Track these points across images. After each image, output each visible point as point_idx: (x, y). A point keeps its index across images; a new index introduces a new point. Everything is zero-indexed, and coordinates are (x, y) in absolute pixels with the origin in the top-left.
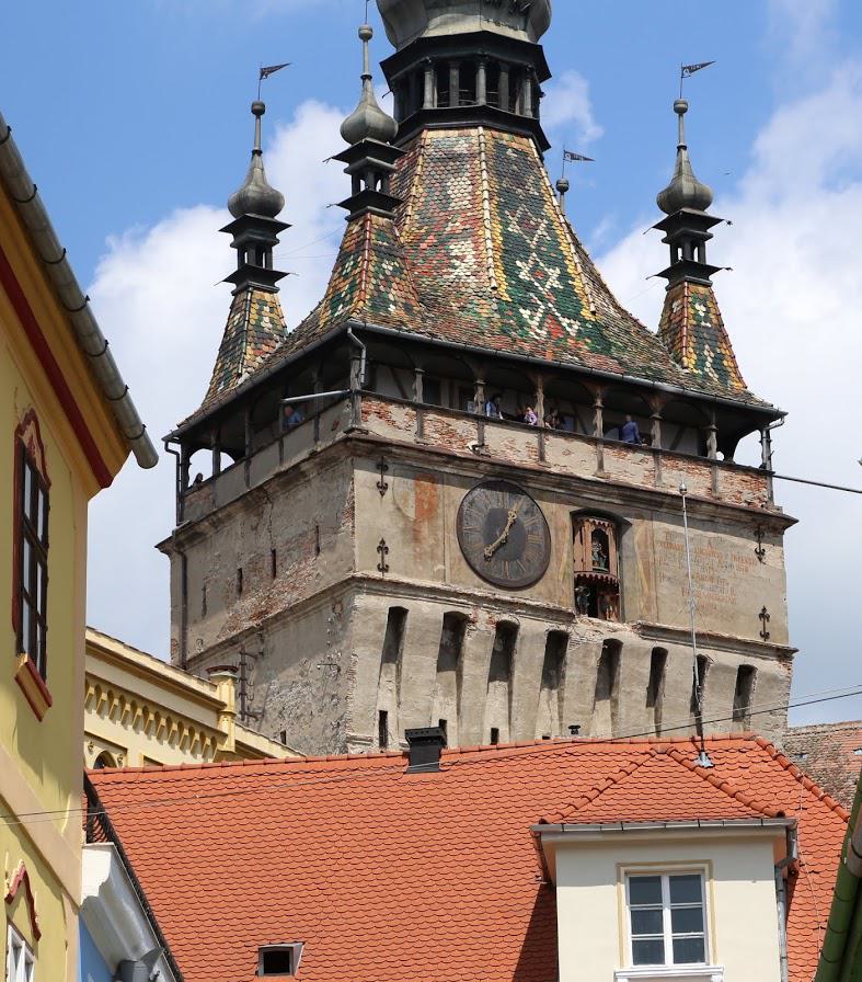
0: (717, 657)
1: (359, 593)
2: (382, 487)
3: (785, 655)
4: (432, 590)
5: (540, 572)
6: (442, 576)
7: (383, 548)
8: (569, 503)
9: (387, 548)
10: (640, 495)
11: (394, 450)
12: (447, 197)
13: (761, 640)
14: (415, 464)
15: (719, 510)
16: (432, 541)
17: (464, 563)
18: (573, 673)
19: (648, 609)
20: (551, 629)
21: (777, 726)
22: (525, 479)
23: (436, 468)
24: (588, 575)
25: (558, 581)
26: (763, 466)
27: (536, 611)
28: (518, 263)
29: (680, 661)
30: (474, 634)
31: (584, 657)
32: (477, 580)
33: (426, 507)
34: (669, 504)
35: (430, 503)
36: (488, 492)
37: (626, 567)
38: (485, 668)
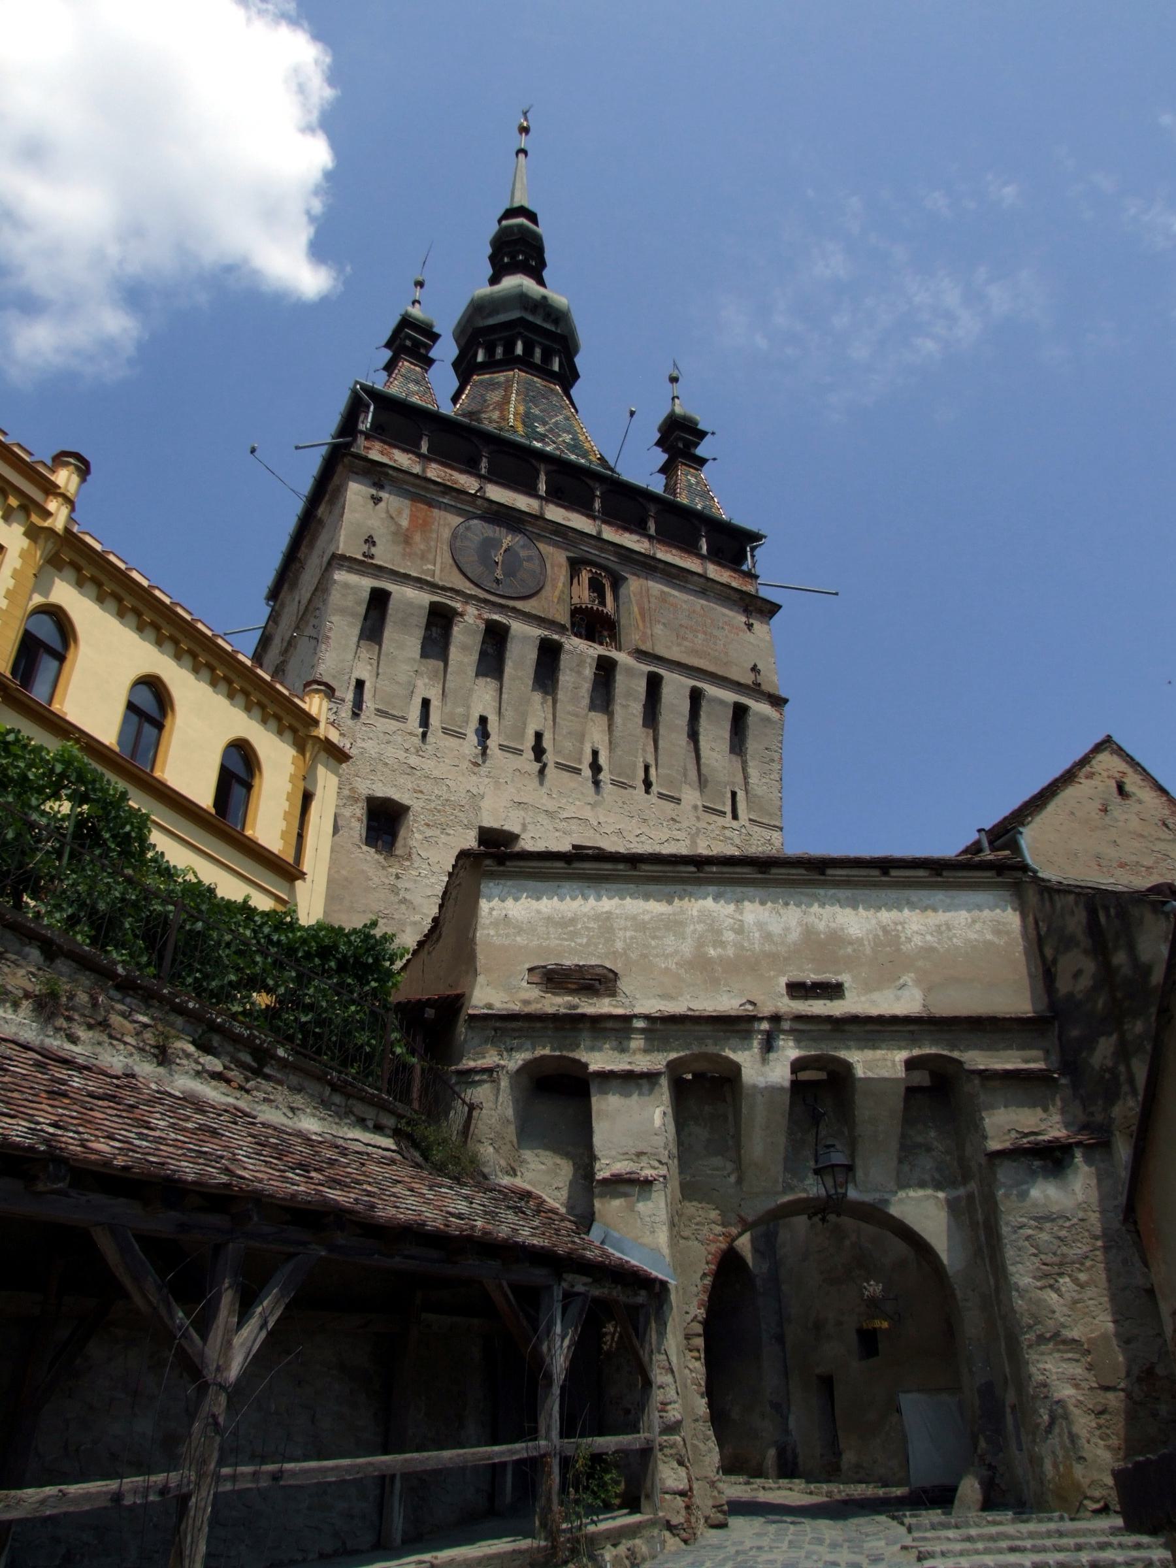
0: (711, 690)
1: (339, 569)
2: (377, 500)
3: (778, 702)
4: (418, 580)
7: (370, 541)
8: (566, 550)
10: (635, 556)
11: (391, 472)
12: (485, 401)
14: (411, 489)
15: (710, 584)
16: (422, 547)
17: (455, 570)
18: (567, 678)
19: (644, 642)
21: (773, 760)
24: (584, 606)
29: (676, 688)
30: (461, 625)
32: (468, 584)
35: (424, 521)
36: (486, 525)
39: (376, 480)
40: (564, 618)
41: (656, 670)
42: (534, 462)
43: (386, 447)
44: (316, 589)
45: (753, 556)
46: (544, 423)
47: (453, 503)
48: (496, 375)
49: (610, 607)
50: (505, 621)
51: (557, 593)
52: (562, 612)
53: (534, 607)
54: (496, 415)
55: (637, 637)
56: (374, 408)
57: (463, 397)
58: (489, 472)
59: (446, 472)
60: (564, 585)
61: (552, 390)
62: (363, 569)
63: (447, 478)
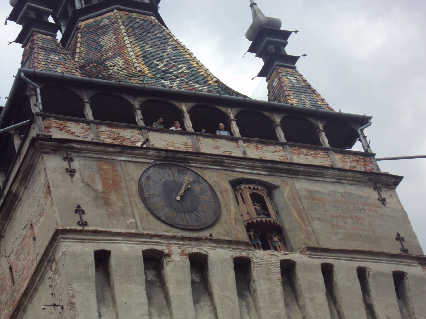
2: (71, 172)
5: (214, 219)
6: (135, 225)
7: (79, 210)
9: (83, 210)
10: (280, 166)
11: (75, 145)
12: (101, 46)
13: (403, 254)
15: (342, 173)
16: (120, 204)
17: (151, 218)
18: (262, 287)
19: (309, 239)
20: (235, 256)
22: (187, 160)
23: (114, 158)
24: (255, 221)
25: (232, 224)
26: (366, 151)
27: (218, 242)
28: (155, 62)
30: (171, 264)
31: (268, 274)
32: (164, 227)
33: (111, 182)
34: (304, 172)
35: (113, 180)
36: (160, 171)
37: (283, 215)
38: (187, 291)
39: (65, 155)
40: (243, 236)
41: (326, 261)
42: (176, 103)
43: (61, 122)
44: (42, 261)
45: (365, 137)
46: (161, 59)
47: (130, 159)
48: (99, 18)
49: (273, 217)
50: (202, 252)
51: (232, 216)
52: (241, 230)
53: (219, 233)
54: (120, 62)
55: (303, 236)
56: (41, 89)
57: (78, 45)
58: (145, 123)
59: (113, 132)
60: (235, 208)
61: (150, 22)
62: (83, 237)
63: (116, 137)
